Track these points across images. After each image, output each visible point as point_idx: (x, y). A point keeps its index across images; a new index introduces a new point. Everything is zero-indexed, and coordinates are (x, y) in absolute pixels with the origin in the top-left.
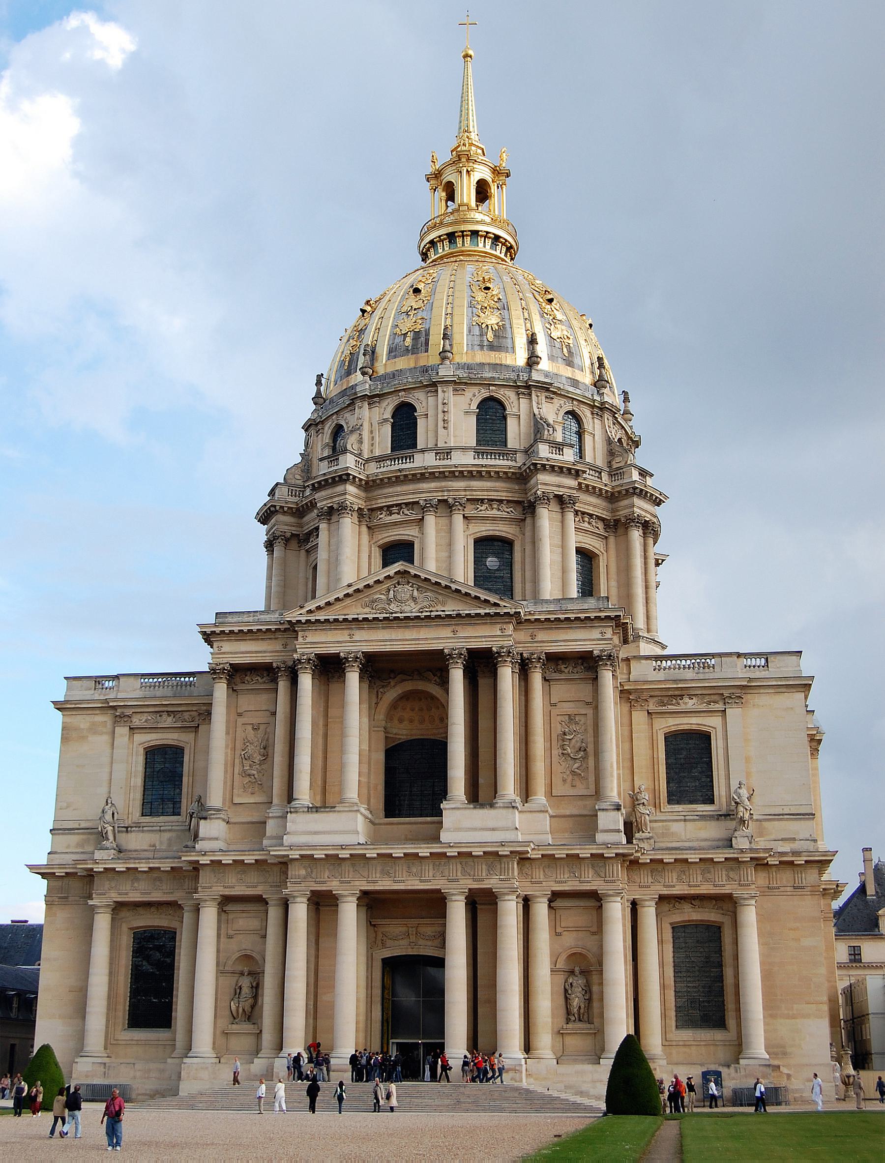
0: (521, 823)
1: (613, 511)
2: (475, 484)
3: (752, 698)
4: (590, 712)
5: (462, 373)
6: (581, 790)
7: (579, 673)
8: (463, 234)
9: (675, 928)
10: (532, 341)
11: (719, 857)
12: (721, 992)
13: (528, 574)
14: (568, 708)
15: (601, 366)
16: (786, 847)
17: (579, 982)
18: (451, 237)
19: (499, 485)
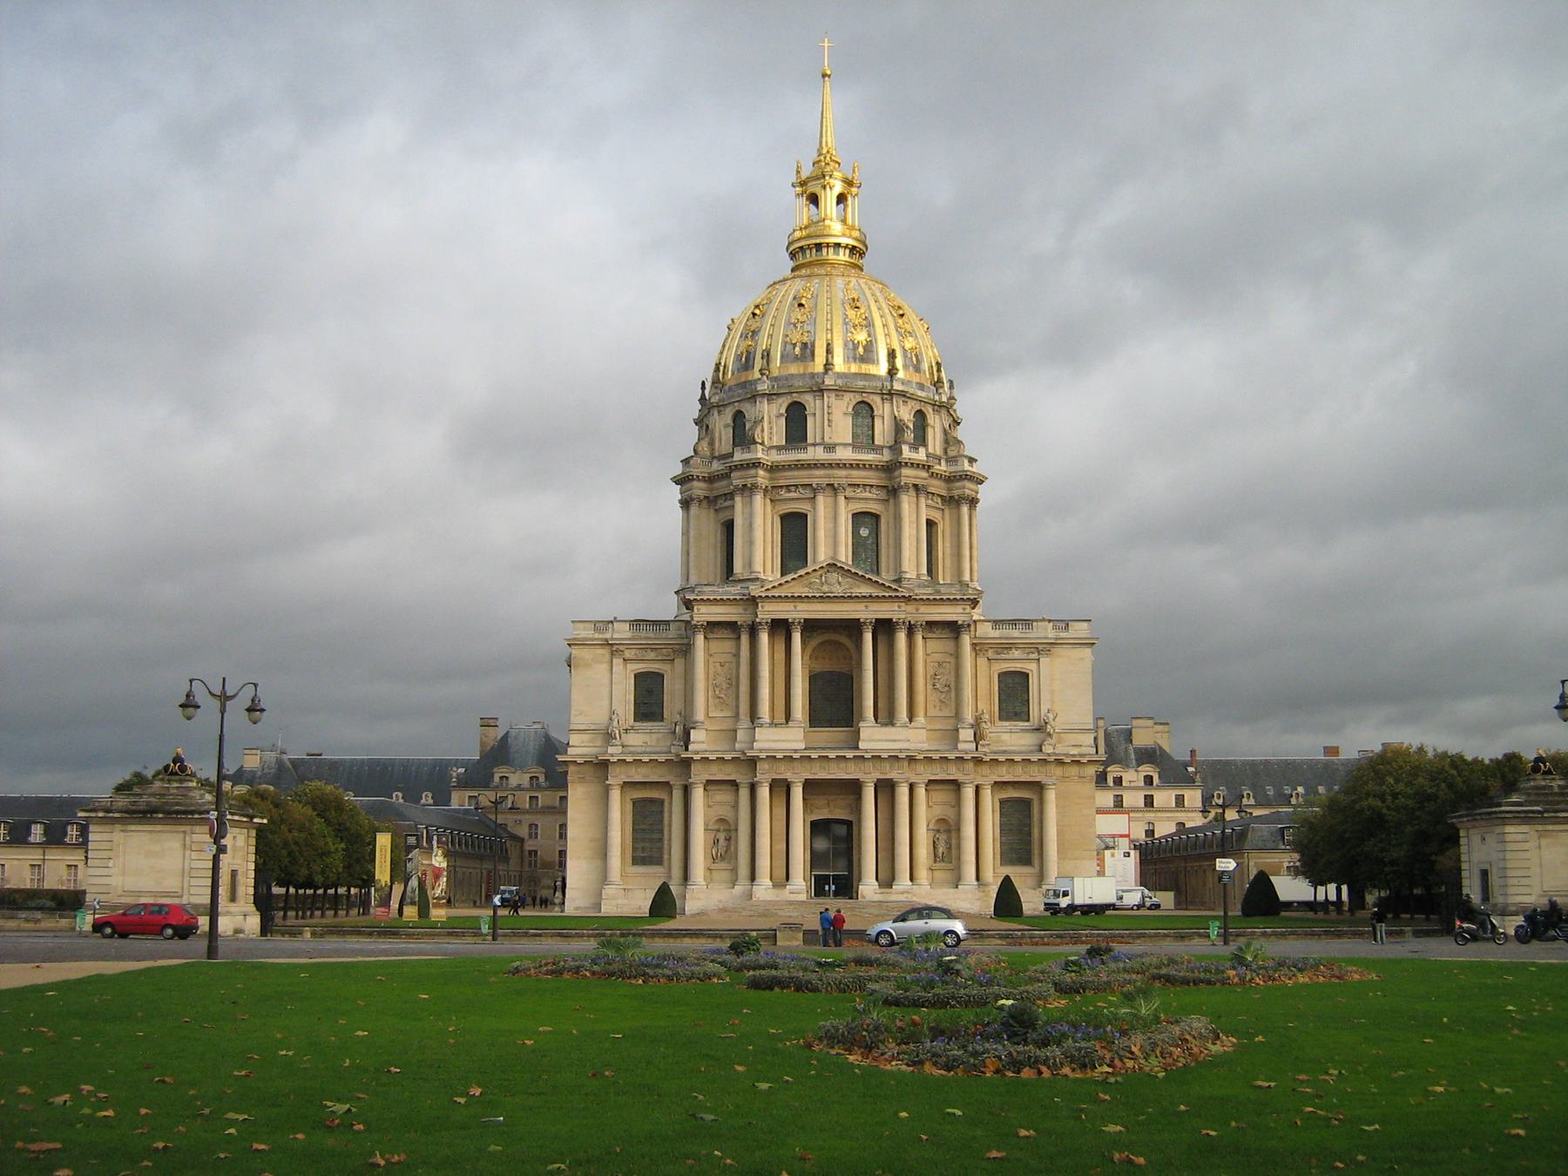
0: (910, 736)
1: (949, 490)
2: (855, 473)
3: (1055, 650)
4: (952, 660)
5: (839, 382)
6: (946, 713)
7: (946, 634)
8: (828, 245)
9: (1002, 802)
10: (892, 355)
11: (1034, 758)
12: (1030, 843)
13: (891, 541)
14: (937, 657)
15: (939, 370)
16: (1074, 751)
17: (943, 837)
18: (819, 247)
19: (870, 473)
